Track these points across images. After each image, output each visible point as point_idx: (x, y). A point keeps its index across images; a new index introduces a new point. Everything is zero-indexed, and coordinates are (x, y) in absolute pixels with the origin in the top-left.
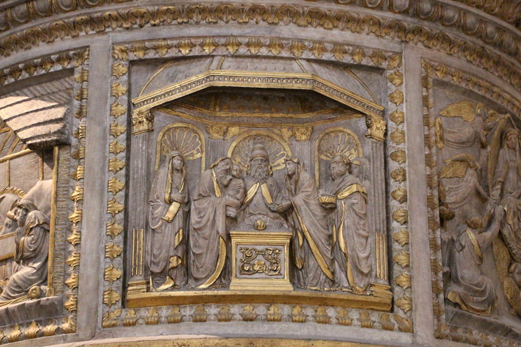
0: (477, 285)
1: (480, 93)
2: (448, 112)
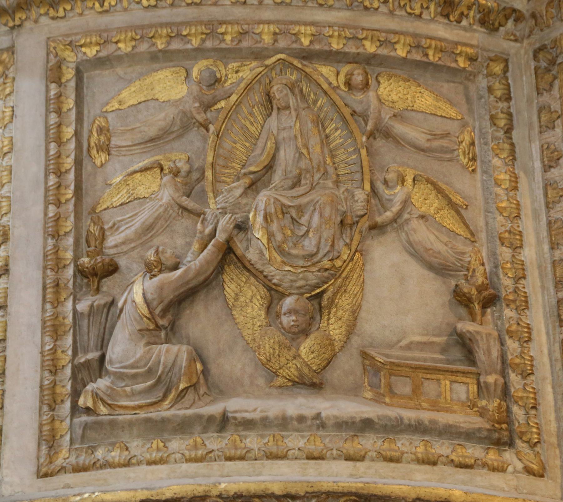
0: (132, 367)
1: (189, 46)
2: (120, 103)
